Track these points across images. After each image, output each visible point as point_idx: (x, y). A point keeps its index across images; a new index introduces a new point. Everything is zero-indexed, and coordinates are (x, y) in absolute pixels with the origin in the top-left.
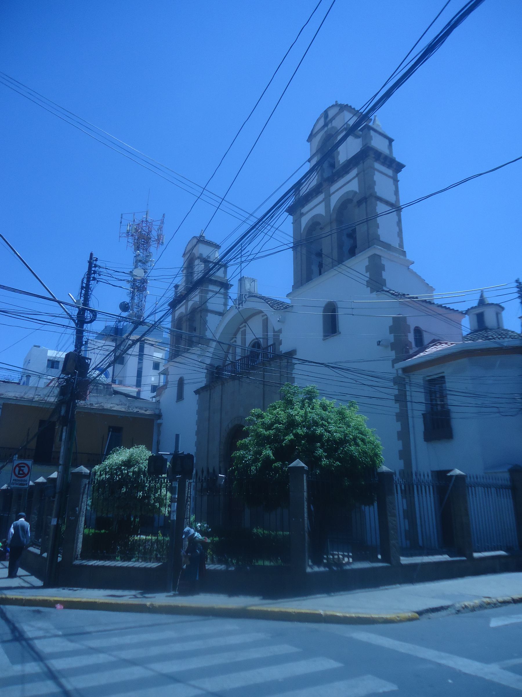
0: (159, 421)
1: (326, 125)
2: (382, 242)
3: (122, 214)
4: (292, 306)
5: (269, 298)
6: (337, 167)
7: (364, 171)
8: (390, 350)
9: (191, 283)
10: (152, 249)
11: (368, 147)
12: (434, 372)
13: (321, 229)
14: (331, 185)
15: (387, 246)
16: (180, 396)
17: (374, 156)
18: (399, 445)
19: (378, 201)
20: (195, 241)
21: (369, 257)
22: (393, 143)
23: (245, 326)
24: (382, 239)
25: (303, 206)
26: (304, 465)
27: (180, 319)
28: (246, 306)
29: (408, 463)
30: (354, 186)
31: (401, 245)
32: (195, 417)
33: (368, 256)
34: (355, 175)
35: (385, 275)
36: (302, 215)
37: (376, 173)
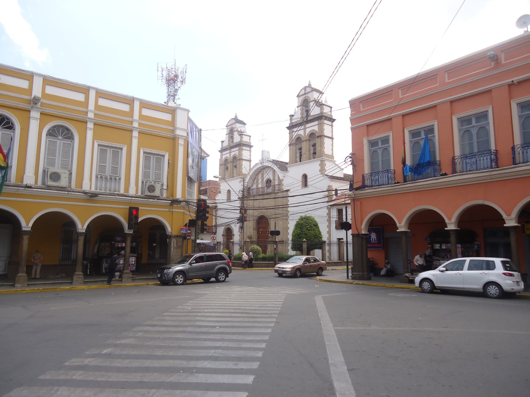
1: (305, 94)
3: (158, 63)
9: (232, 142)
12: (340, 207)
13: (302, 141)
15: (328, 156)
18: (327, 230)
20: (234, 121)
22: (332, 108)
25: (294, 128)
27: (226, 160)
29: (330, 236)
30: (316, 128)
31: (332, 154)
34: (317, 124)
35: (327, 168)
36: (293, 132)
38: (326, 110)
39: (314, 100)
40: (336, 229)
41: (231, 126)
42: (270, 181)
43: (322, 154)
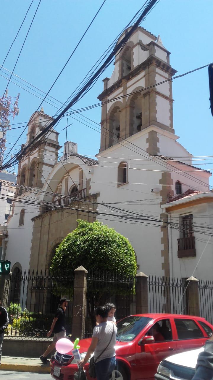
0: (6, 239)
2: (158, 122)
4: (99, 163)
5: (84, 157)
6: (132, 70)
7: (149, 74)
8: (159, 195)
10: (10, 118)
11: (152, 57)
12: (185, 211)
13: (120, 111)
14: (128, 82)
15: (162, 126)
16: (21, 223)
17: (156, 64)
18: (162, 260)
19: (157, 94)
21: (149, 133)
23: (68, 175)
24: (158, 121)
25: (109, 95)
26: (84, 269)
28: (68, 161)
29: (167, 272)
30: (142, 84)
32: (32, 237)
33: (149, 131)
34: (143, 76)
35: (159, 145)
36: (108, 101)
37: (157, 75)
38: (160, 55)
39: (139, 42)
40: (178, 257)
41: (34, 122)
42: (77, 190)
43: (153, 121)
